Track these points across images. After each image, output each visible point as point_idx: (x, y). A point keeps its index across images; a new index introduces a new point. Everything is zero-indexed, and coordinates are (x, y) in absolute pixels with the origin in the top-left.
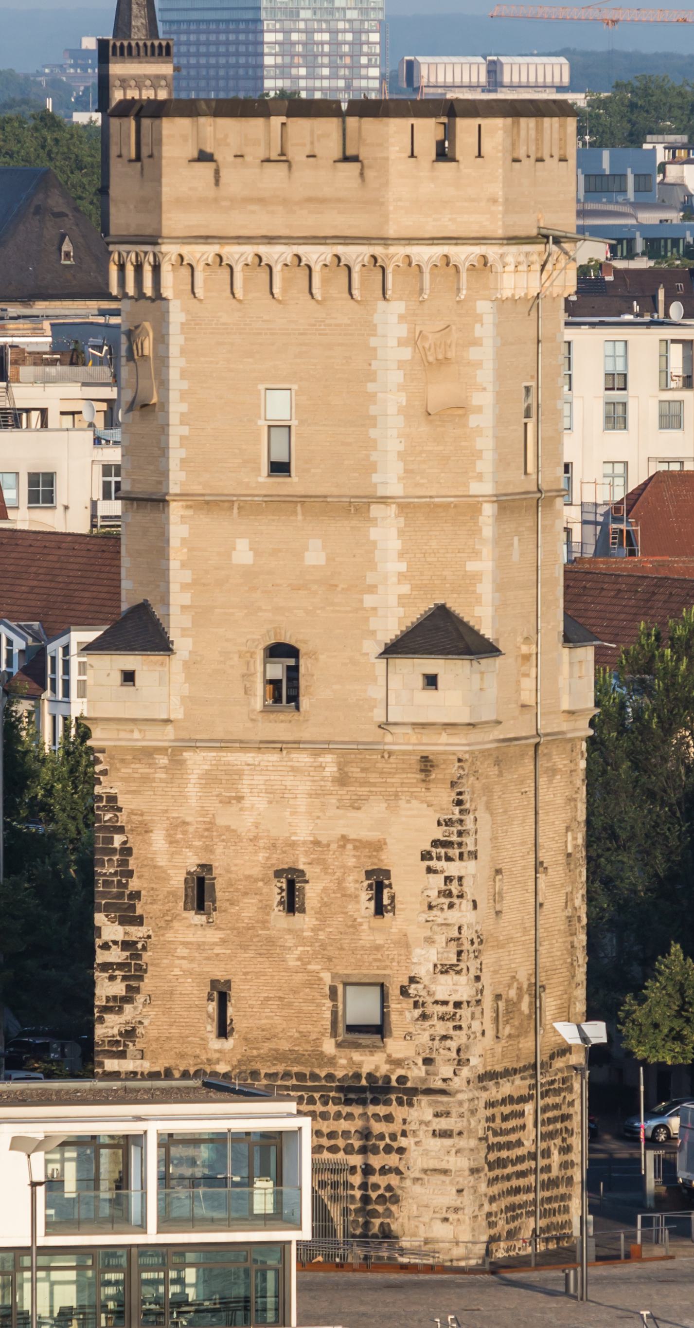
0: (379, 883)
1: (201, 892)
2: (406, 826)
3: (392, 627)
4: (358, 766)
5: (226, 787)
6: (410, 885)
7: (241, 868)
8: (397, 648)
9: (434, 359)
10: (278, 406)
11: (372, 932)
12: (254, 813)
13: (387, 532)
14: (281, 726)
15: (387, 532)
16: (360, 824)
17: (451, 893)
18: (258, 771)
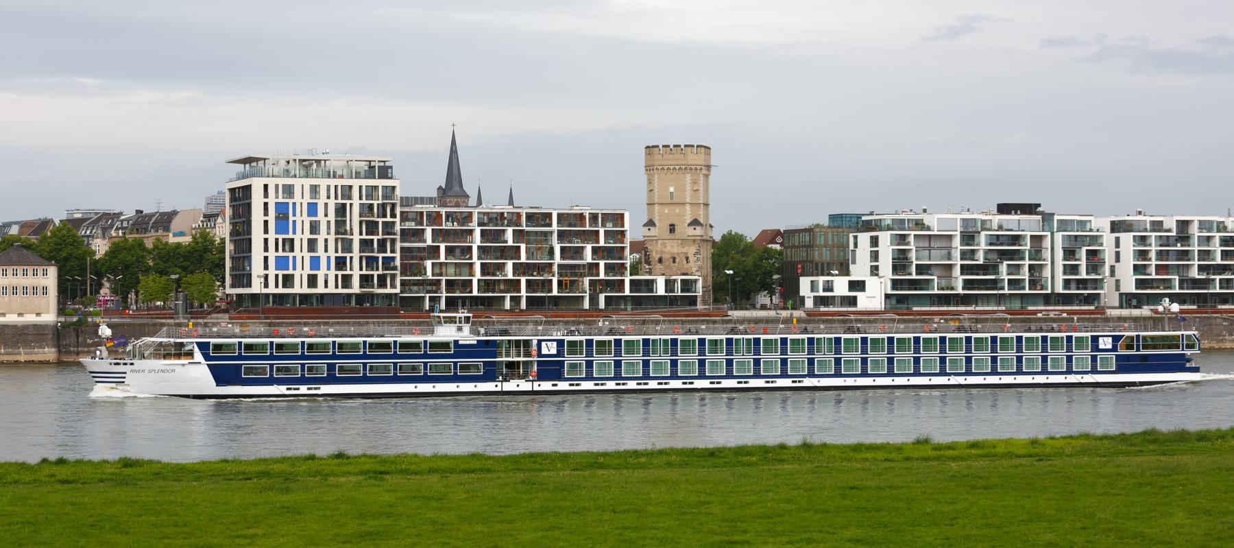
0: (687, 258)
1: (660, 260)
2: (691, 250)
3: (688, 221)
4: (684, 242)
5: (664, 245)
6: (692, 259)
7: (666, 257)
8: (690, 225)
9: (695, 182)
10: (672, 189)
11: (686, 266)
12: (668, 249)
13: (688, 207)
14: (672, 236)
15: (688, 207)
16: (684, 250)
17: (698, 260)
18: (669, 243)
